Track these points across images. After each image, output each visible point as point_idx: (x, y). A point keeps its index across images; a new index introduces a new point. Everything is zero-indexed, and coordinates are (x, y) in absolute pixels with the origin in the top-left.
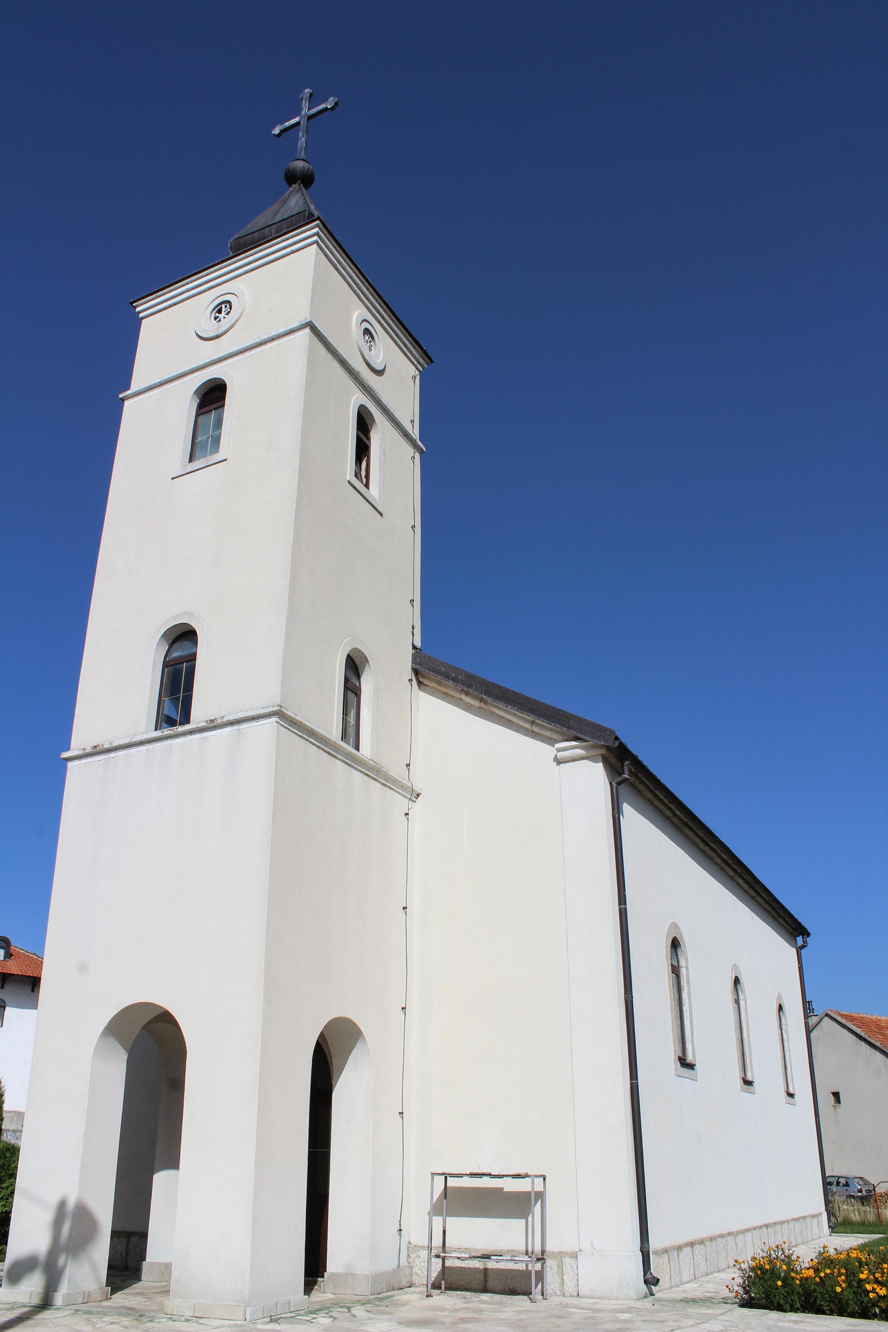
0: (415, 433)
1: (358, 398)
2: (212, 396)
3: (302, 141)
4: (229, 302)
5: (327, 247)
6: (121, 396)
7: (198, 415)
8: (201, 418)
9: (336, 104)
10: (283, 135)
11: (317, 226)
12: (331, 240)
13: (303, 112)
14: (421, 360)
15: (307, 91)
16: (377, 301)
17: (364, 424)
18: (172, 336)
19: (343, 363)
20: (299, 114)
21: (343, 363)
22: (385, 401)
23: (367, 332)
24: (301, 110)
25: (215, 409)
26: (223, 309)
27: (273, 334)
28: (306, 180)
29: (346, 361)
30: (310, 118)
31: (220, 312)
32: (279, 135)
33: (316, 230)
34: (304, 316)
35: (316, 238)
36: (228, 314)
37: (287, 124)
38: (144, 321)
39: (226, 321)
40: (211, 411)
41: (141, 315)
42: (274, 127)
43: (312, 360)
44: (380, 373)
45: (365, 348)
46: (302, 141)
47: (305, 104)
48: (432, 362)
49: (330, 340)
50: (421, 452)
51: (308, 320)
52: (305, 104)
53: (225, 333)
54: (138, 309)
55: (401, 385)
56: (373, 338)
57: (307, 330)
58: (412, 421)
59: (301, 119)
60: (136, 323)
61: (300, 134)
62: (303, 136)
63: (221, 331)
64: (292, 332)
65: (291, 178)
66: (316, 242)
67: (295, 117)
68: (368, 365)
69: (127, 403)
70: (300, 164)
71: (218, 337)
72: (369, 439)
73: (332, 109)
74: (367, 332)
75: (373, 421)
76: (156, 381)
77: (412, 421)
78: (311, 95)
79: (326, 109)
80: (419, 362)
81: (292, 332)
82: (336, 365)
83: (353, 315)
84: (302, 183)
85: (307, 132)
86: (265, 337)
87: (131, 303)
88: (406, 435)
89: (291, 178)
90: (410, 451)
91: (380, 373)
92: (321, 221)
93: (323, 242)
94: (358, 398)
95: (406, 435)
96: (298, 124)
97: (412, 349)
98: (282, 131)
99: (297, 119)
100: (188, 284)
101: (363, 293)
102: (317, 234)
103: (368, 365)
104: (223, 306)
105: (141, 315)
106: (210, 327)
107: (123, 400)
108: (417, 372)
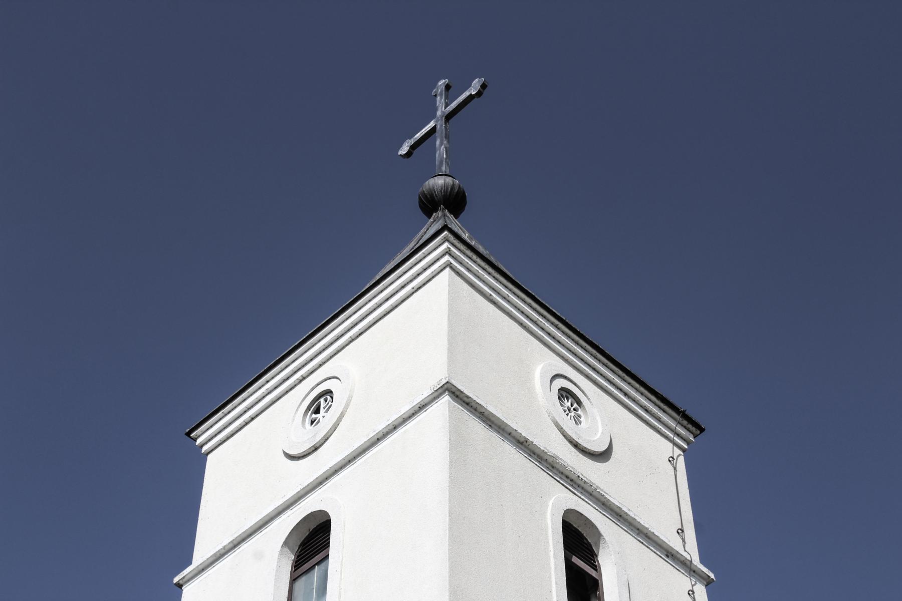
0: (691, 551)
1: (560, 500)
2: (312, 543)
3: (441, 149)
4: (329, 392)
5: (469, 270)
6: (176, 580)
7: (293, 580)
8: (300, 584)
9: (484, 86)
10: (416, 152)
11: (446, 240)
12: (474, 257)
13: (439, 113)
14: (680, 430)
15: (441, 82)
16: (577, 343)
17: (578, 542)
18: (248, 468)
19: (522, 444)
20: (433, 116)
21: (522, 444)
22: (615, 499)
23: (564, 394)
24: (436, 109)
25: (318, 564)
26: (322, 407)
27: (393, 417)
28: (455, 202)
29: (527, 441)
30: (449, 117)
31: (317, 411)
32: (409, 154)
33: (446, 245)
34: (439, 377)
35: (447, 258)
36: (327, 411)
37: (418, 135)
38: (209, 457)
39: (326, 419)
40: (313, 567)
41: (205, 449)
42: (400, 146)
43: (457, 443)
44: (603, 456)
45: (568, 424)
46: (441, 149)
47: (440, 101)
48: (702, 430)
49: (491, 409)
50: (708, 583)
51: (444, 381)
52: (440, 101)
53: (326, 439)
54: (199, 441)
55: (646, 471)
56: (579, 403)
57: (446, 398)
58: (680, 532)
59: (437, 121)
60: (196, 463)
61: (438, 142)
62: (441, 144)
63: (318, 438)
64: (422, 407)
65: (429, 204)
66: (449, 265)
67: (429, 123)
68: (576, 445)
69: (187, 590)
70: (440, 181)
71: (315, 448)
72: (596, 568)
73: (479, 94)
74: (564, 394)
75: (599, 535)
76: (226, 541)
77: (680, 532)
78: (448, 87)
79: (471, 97)
80: (678, 435)
81: (422, 407)
82: (509, 449)
83: (526, 367)
84: (446, 207)
85: (447, 137)
86: (381, 426)
87: (188, 434)
88: (670, 555)
89: (429, 204)
90: (684, 582)
91: (603, 456)
92: (451, 231)
93: (461, 263)
94: (560, 500)
95: (670, 555)
96: (433, 130)
97: (660, 414)
98: (413, 147)
99: (432, 124)
100: (268, 382)
101: (549, 334)
102: (448, 252)
103: (576, 445)
104: (322, 400)
105: (205, 448)
106: (302, 436)
107: (180, 586)
108: (678, 452)
